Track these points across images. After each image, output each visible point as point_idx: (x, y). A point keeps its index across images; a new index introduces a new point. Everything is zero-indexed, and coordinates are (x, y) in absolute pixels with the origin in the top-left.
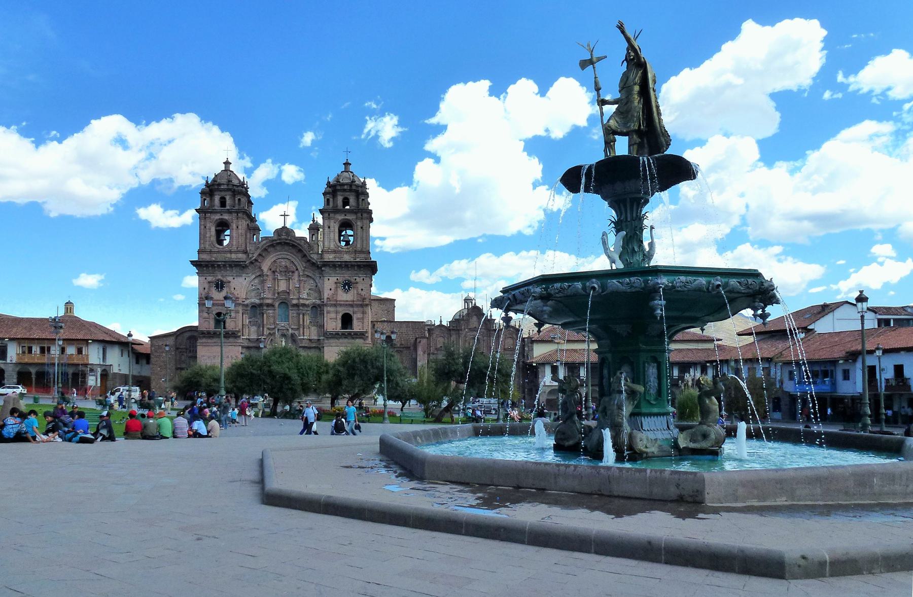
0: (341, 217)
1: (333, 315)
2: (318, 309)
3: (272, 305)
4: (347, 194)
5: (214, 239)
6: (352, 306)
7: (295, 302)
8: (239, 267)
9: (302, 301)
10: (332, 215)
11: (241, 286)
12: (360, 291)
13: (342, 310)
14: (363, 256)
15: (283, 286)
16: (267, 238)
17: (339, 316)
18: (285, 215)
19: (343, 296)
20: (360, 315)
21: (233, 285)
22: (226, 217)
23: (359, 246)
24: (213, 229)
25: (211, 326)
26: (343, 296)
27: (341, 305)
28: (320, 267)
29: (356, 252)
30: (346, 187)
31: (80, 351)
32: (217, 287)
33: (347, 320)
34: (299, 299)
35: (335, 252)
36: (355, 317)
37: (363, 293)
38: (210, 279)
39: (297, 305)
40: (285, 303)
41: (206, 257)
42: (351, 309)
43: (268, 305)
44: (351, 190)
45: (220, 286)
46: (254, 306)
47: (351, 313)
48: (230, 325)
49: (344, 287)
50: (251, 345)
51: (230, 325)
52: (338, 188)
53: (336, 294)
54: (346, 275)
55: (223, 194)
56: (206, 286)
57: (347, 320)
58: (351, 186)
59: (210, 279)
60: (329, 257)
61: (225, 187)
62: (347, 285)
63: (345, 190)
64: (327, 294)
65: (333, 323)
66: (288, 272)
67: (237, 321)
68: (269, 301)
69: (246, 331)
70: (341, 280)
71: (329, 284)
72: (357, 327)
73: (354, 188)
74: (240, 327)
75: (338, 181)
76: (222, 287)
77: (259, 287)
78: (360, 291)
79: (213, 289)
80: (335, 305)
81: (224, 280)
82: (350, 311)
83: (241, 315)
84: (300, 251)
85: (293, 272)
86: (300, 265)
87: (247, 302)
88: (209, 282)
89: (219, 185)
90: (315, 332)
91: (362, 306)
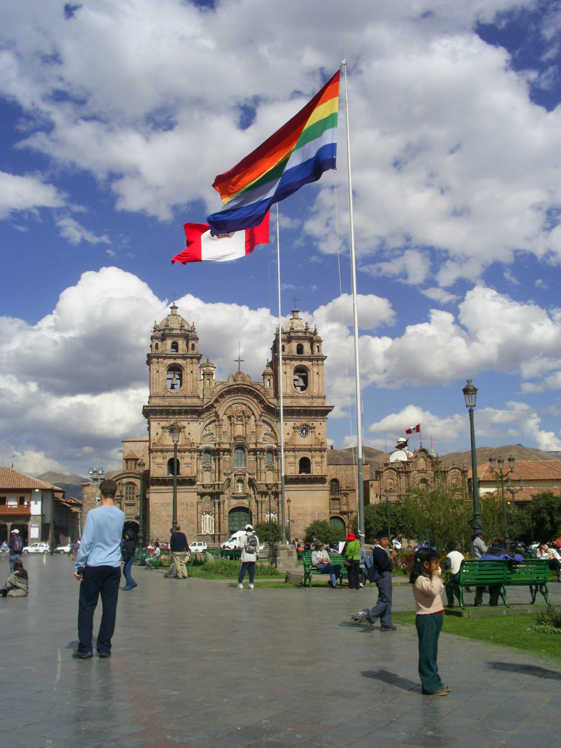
1: (292, 460)
3: (229, 451)
4: (301, 342)
6: (310, 450)
7: (252, 446)
9: (259, 446)
11: (195, 431)
12: (317, 435)
15: (239, 430)
17: (298, 460)
19: (168, 440)
21: (187, 430)
22: (179, 361)
23: (315, 391)
27: (299, 450)
29: (312, 397)
30: (300, 334)
31: (21, 501)
33: (305, 464)
34: (256, 444)
35: (292, 397)
36: (313, 461)
37: (321, 437)
38: (163, 424)
39: (255, 451)
40: (241, 447)
41: (156, 401)
42: (310, 454)
43: (225, 450)
44: (305, 338)
47: (310, 458)
48: (185, 471)
49: (302, 431)
51: (185, 471)
52: (292, 334)
54: (304, 421)
55: (175, 339)
56: (160, 431)
58: (305, 333)
59: (163, 424)
61: (178, 332)
62: (306, 429)
63: (299, 338)
65: (289, 466)
66: (244, 417)
68: (227, 446)
69: (200, 476)
70: (298, 424)
73: (308, 335)
74: (195, 471)
75: (292, 329)
77: (214, 432)
78: (317, 435)
79: (167, 434)
80: (294, 450)
82: (308, 455)
83: (196, 459)
84: (257, 397)
85: (249, 417)
86: (257, 409)
88: (163, 428)
89: (172, 329)
90: (271, 477)
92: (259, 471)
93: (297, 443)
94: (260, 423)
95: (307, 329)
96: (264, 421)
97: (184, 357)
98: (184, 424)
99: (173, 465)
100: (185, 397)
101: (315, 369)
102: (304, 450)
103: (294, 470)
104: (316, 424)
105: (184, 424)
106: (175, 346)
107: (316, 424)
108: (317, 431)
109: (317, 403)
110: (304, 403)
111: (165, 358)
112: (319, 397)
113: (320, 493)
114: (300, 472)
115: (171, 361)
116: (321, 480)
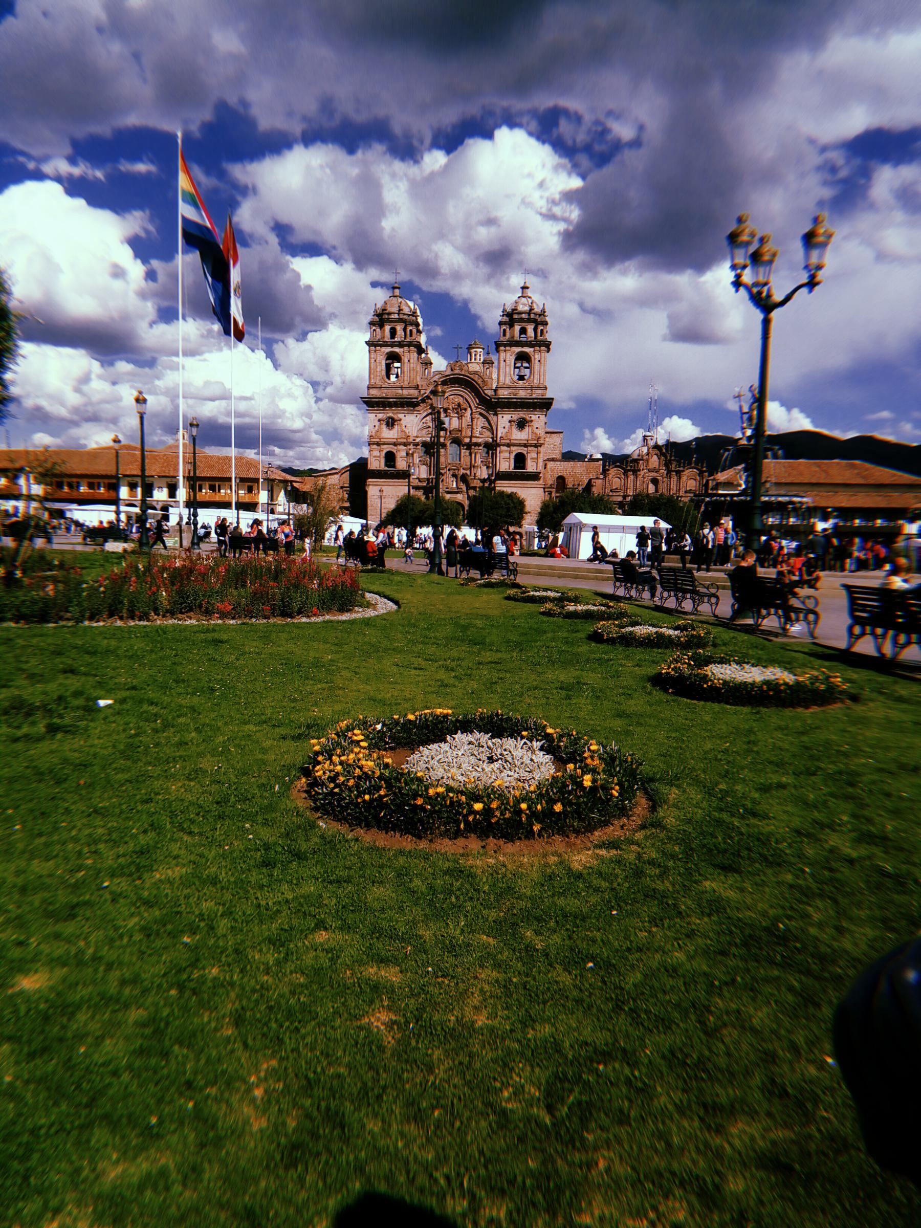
1: (507, 455)
2: (491, 447)
5: (384, 373)
7: (467, 440)
8: (410, 404)
9: (474, 440)
11: (413, 424)
13: (516, 450)
14: (540, 391)
16: (440, 373)
17: (513, 456)
20: (534, 455)
21: (403, 423)
22: (397, 349)
24: (384, 363)
26: (520, 436)
29: (532, 388)
30: (523, 316)
32: (387, 424)
33: (520, 460)
34: (471, 437)
35: (509, 388)
36: (529, 457)
37: (538, 432)
38: (380, 416)
41: (374, 392)
44: (529, 321)
45: (391, 423)
50: (420, 484)
51: (401, 464)
52: (516, 316)
53: (510, 432)
56: (377, 424)
57: (520, 460)
58: (529, 314)
59: (380, 416)
60: (504, 393)
61: (396, 316)
62: (522, 424)
63: (521, 320)
64: (501, 432)
65: (505, 463)
71: (504, 421)
72: (531, 467)
73: (532, 316)
76: (393, 425)
79: (384, 427)
80: (508, 445)
81: (395, 417)
82: (523, 450)
86: (473, 401)
87: (418, 440)
89: (390, 314)
91: (536, 446)
92: (472, 466)
93: (514, 437)
94: (477, 416)
95: (531, 309)
96: (481, 414)
97: (401, 345)
98: (401, 416)
99: (390, 458)
100: (402, 388)
101: (537, 356)
102: (520, 445)
104: (533, 417)
105: (401, 416)
106: (393, 332)
107: (533, 417)
108: (535, 425)
109: (537, 394)
110: (522, 394)
111: (381, 346)
112: (538, 388)
113: (534, 491)
114: (515, 468)
115: (389, 349)
116: (535, 477)
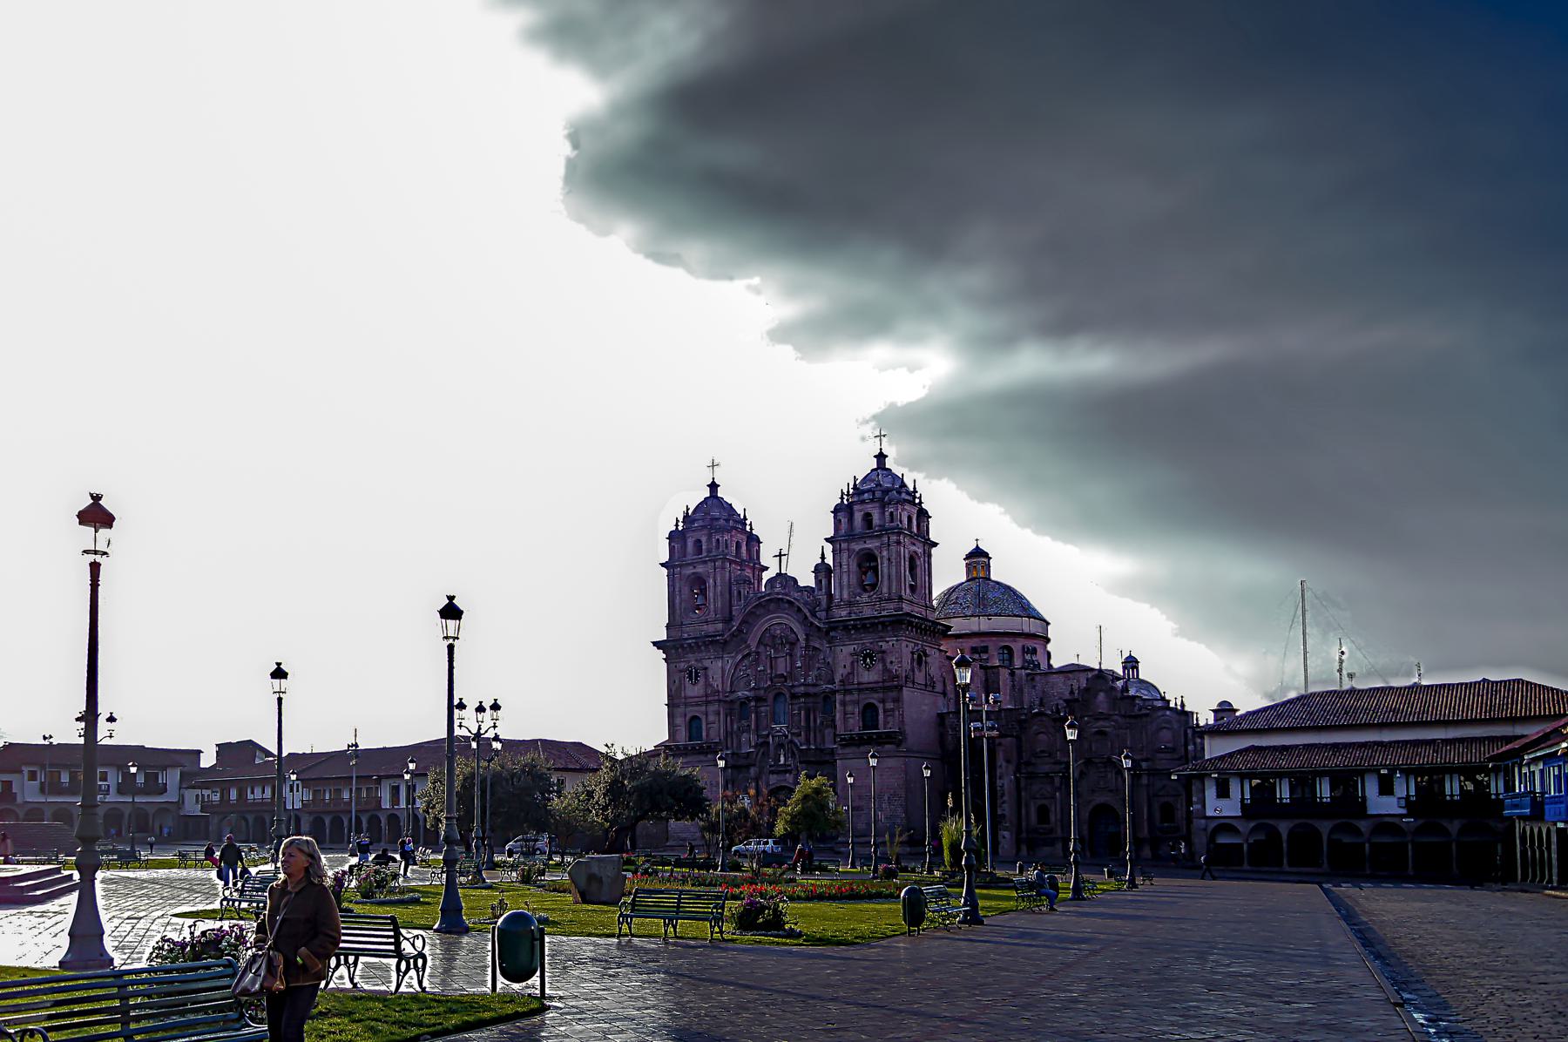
0: (857, 547)
10: (844, 545)
15: (782, 666)
18: (780, 555)
23: (885, 590)
25: (682, 738)
28: (834, 630)
36: (880, 706)
45: (693, 675)
46: (744, 703)
54: (867, 640)
57: (869, 713)
60: (842, 614)
64: (840, 673)
65: (848, 720)
67: (714, 727)
82: (873, 699)
91: (890, 689)
103: (855, 725)
105: (707, 663)
110: (868, 612)
